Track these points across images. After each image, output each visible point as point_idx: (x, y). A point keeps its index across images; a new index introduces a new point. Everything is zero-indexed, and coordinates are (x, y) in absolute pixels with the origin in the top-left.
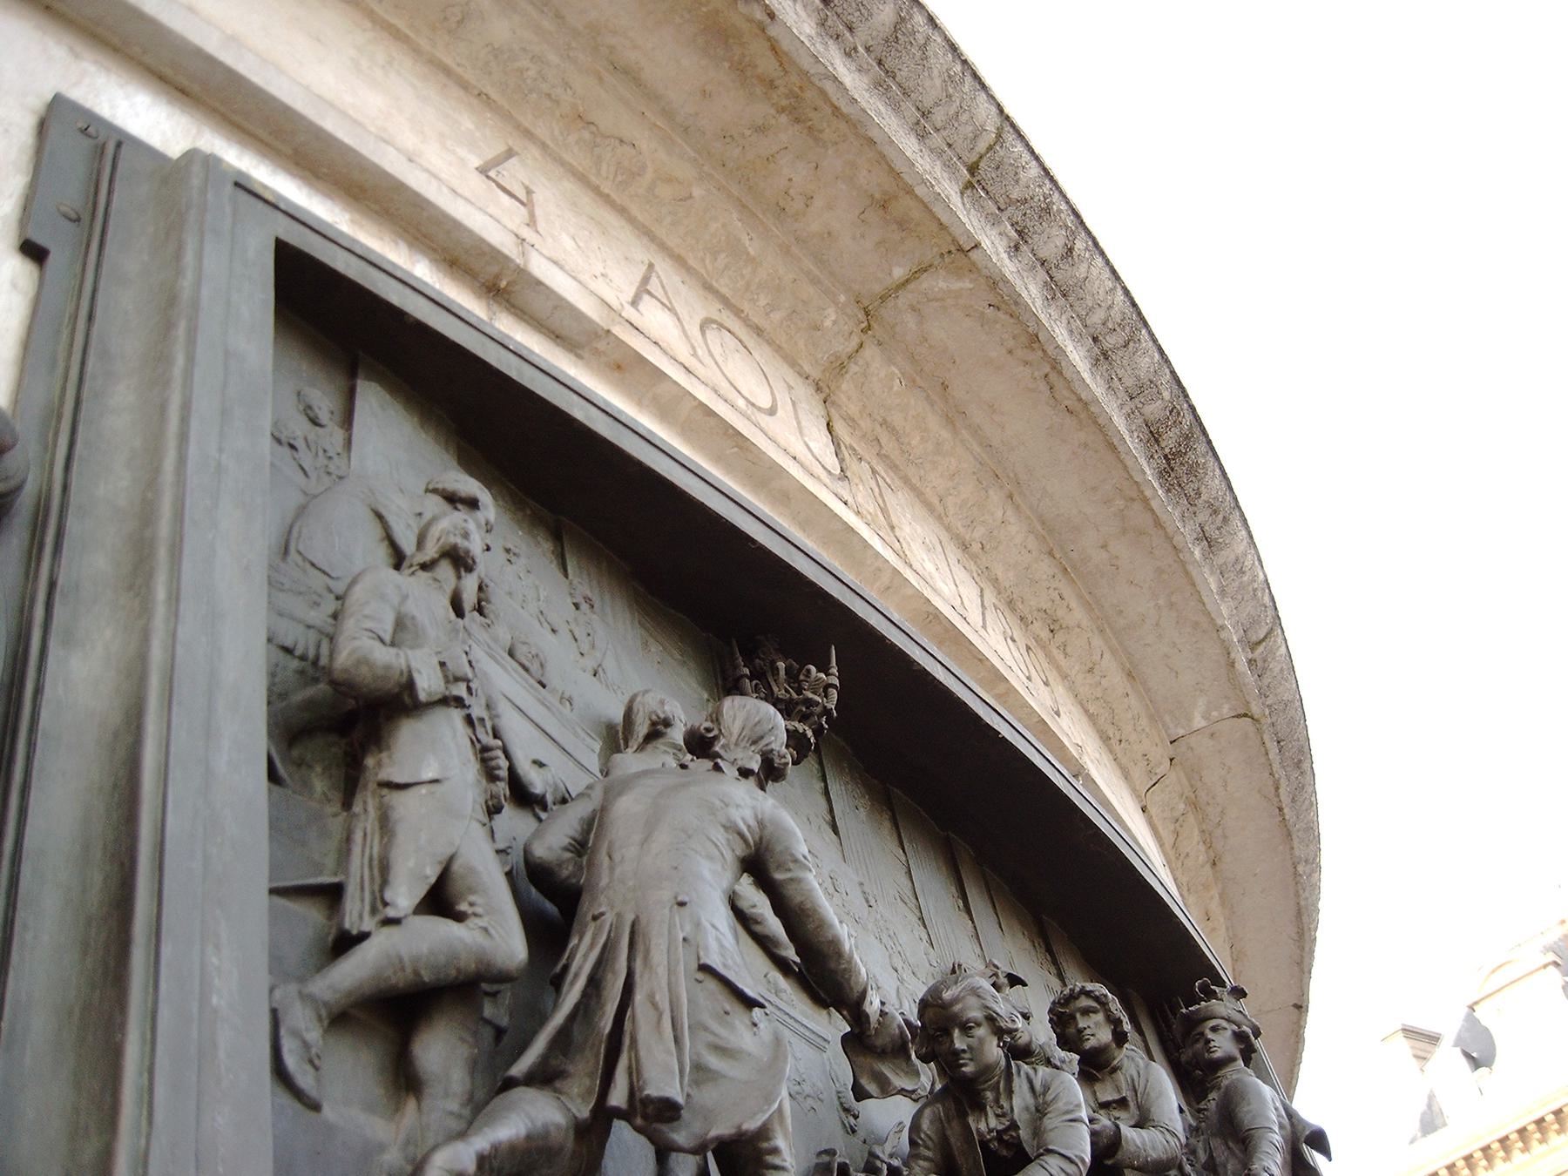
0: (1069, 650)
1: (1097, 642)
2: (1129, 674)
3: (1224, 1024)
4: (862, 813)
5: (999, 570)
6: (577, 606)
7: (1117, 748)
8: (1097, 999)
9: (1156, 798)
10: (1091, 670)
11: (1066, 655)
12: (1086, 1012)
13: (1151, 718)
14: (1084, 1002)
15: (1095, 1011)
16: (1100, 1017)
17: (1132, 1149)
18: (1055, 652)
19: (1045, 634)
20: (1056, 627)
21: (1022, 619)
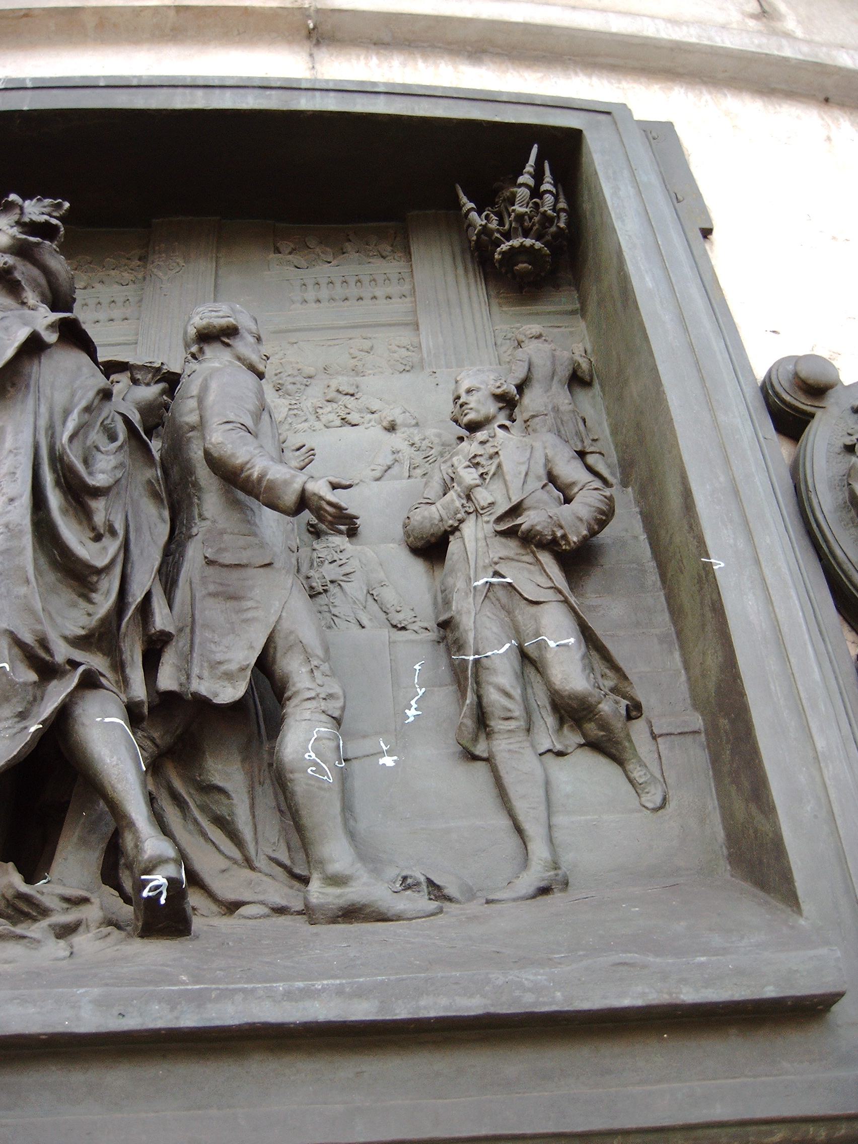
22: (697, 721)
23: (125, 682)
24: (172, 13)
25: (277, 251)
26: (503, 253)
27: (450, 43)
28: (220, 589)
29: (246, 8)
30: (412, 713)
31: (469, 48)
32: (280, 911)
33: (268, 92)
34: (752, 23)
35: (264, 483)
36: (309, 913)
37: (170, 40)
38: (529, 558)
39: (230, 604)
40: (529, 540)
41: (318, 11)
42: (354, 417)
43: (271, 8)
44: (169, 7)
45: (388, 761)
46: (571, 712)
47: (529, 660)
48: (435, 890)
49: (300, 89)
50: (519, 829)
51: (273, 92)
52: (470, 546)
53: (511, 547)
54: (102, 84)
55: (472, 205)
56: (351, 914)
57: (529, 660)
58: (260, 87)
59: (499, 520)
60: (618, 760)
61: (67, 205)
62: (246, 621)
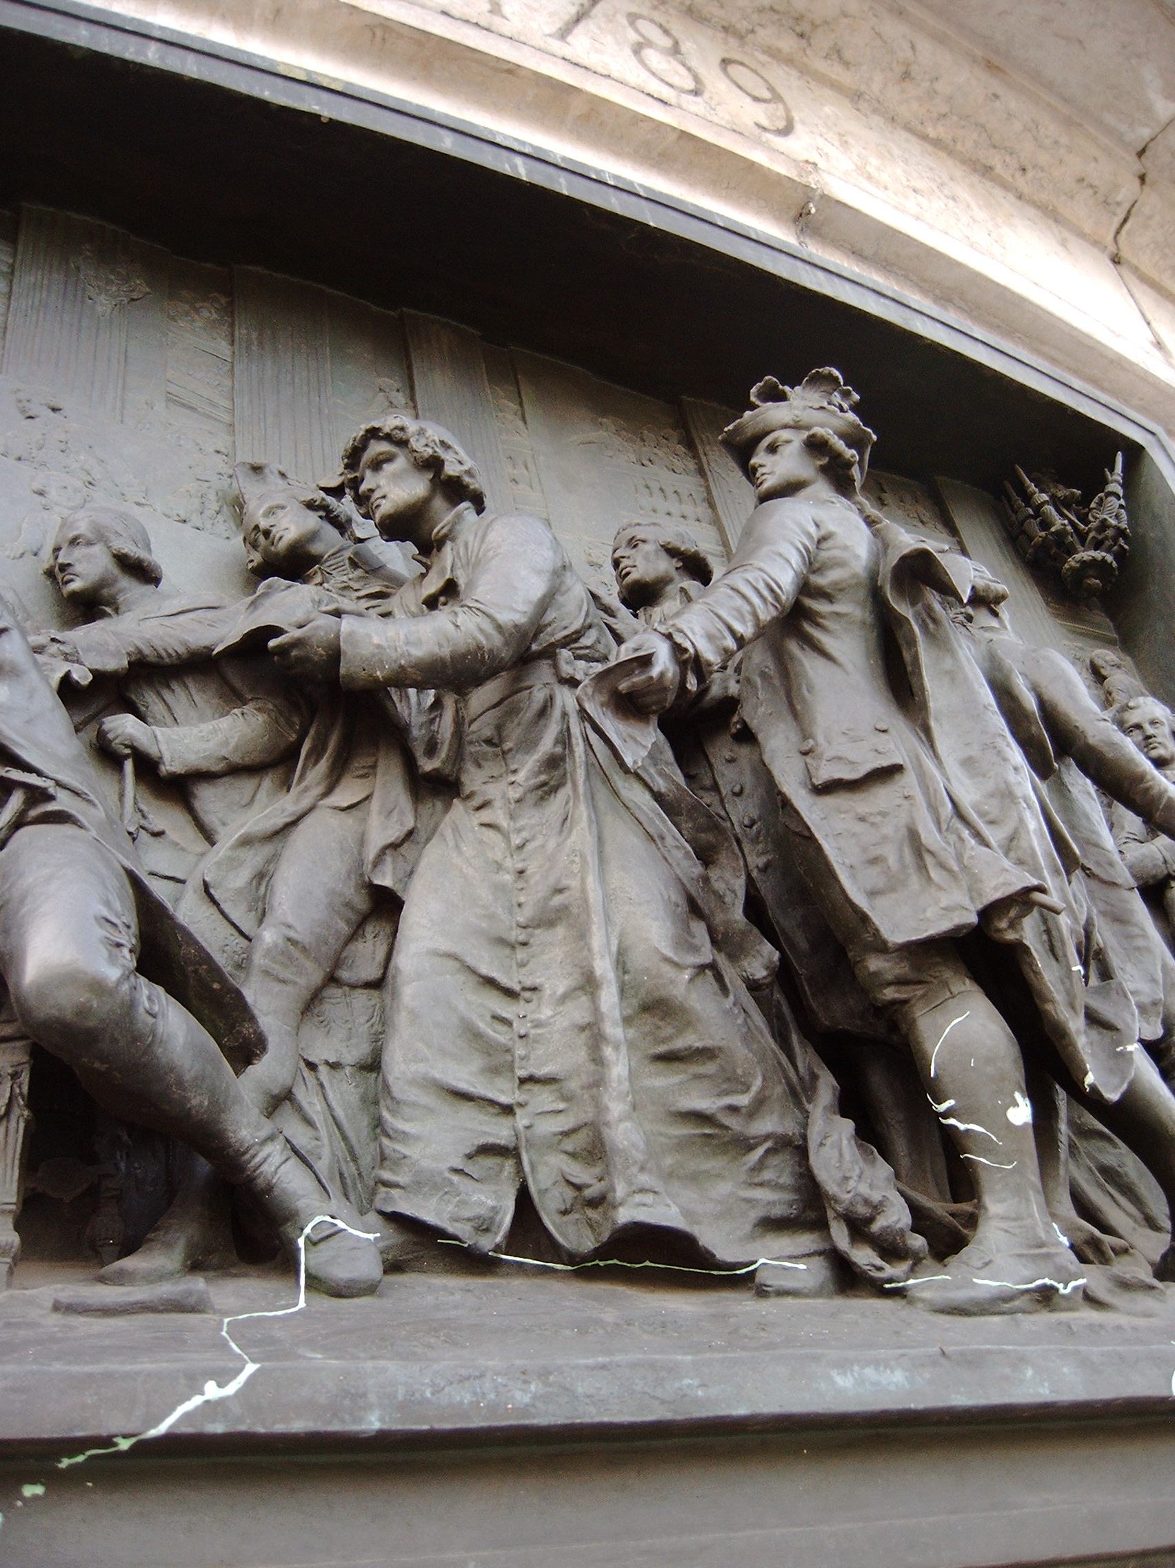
0: (848, 54)
1: (893, 29)
2: (990, 66)
3: (784, 435)
4: (103, 304)
7: (1021, 182)
8: (388, 438)
9: (1136, 244)
10: (906, 76)
11: (847, 65)
12: (377, 465)
13: (1068, 122)
14: (377, 448)
15: (390, 459)
16: (401, 462)
17: (366, 651)
18: (820, 65)
19: (787, 43)
20: (805, 27)
21: (726, 29)
24: (673, 137)
26: (1083, 562)
27: (925, 281)
28: (1109, 908)
29: (753, 163)
31: (937, 292)
33: (882, 300)
35: (1164, 801)
37: (653, 166)
39: (1116, 926)
41: (824, 197)
43: (778, 174)
44: (674, 129)
49: (909, 307)
51: (887, 302)
54: (720, 223)
55: (1045, 497)
58: (874, 291)
61: (856, 397)
62: (1138, 949)
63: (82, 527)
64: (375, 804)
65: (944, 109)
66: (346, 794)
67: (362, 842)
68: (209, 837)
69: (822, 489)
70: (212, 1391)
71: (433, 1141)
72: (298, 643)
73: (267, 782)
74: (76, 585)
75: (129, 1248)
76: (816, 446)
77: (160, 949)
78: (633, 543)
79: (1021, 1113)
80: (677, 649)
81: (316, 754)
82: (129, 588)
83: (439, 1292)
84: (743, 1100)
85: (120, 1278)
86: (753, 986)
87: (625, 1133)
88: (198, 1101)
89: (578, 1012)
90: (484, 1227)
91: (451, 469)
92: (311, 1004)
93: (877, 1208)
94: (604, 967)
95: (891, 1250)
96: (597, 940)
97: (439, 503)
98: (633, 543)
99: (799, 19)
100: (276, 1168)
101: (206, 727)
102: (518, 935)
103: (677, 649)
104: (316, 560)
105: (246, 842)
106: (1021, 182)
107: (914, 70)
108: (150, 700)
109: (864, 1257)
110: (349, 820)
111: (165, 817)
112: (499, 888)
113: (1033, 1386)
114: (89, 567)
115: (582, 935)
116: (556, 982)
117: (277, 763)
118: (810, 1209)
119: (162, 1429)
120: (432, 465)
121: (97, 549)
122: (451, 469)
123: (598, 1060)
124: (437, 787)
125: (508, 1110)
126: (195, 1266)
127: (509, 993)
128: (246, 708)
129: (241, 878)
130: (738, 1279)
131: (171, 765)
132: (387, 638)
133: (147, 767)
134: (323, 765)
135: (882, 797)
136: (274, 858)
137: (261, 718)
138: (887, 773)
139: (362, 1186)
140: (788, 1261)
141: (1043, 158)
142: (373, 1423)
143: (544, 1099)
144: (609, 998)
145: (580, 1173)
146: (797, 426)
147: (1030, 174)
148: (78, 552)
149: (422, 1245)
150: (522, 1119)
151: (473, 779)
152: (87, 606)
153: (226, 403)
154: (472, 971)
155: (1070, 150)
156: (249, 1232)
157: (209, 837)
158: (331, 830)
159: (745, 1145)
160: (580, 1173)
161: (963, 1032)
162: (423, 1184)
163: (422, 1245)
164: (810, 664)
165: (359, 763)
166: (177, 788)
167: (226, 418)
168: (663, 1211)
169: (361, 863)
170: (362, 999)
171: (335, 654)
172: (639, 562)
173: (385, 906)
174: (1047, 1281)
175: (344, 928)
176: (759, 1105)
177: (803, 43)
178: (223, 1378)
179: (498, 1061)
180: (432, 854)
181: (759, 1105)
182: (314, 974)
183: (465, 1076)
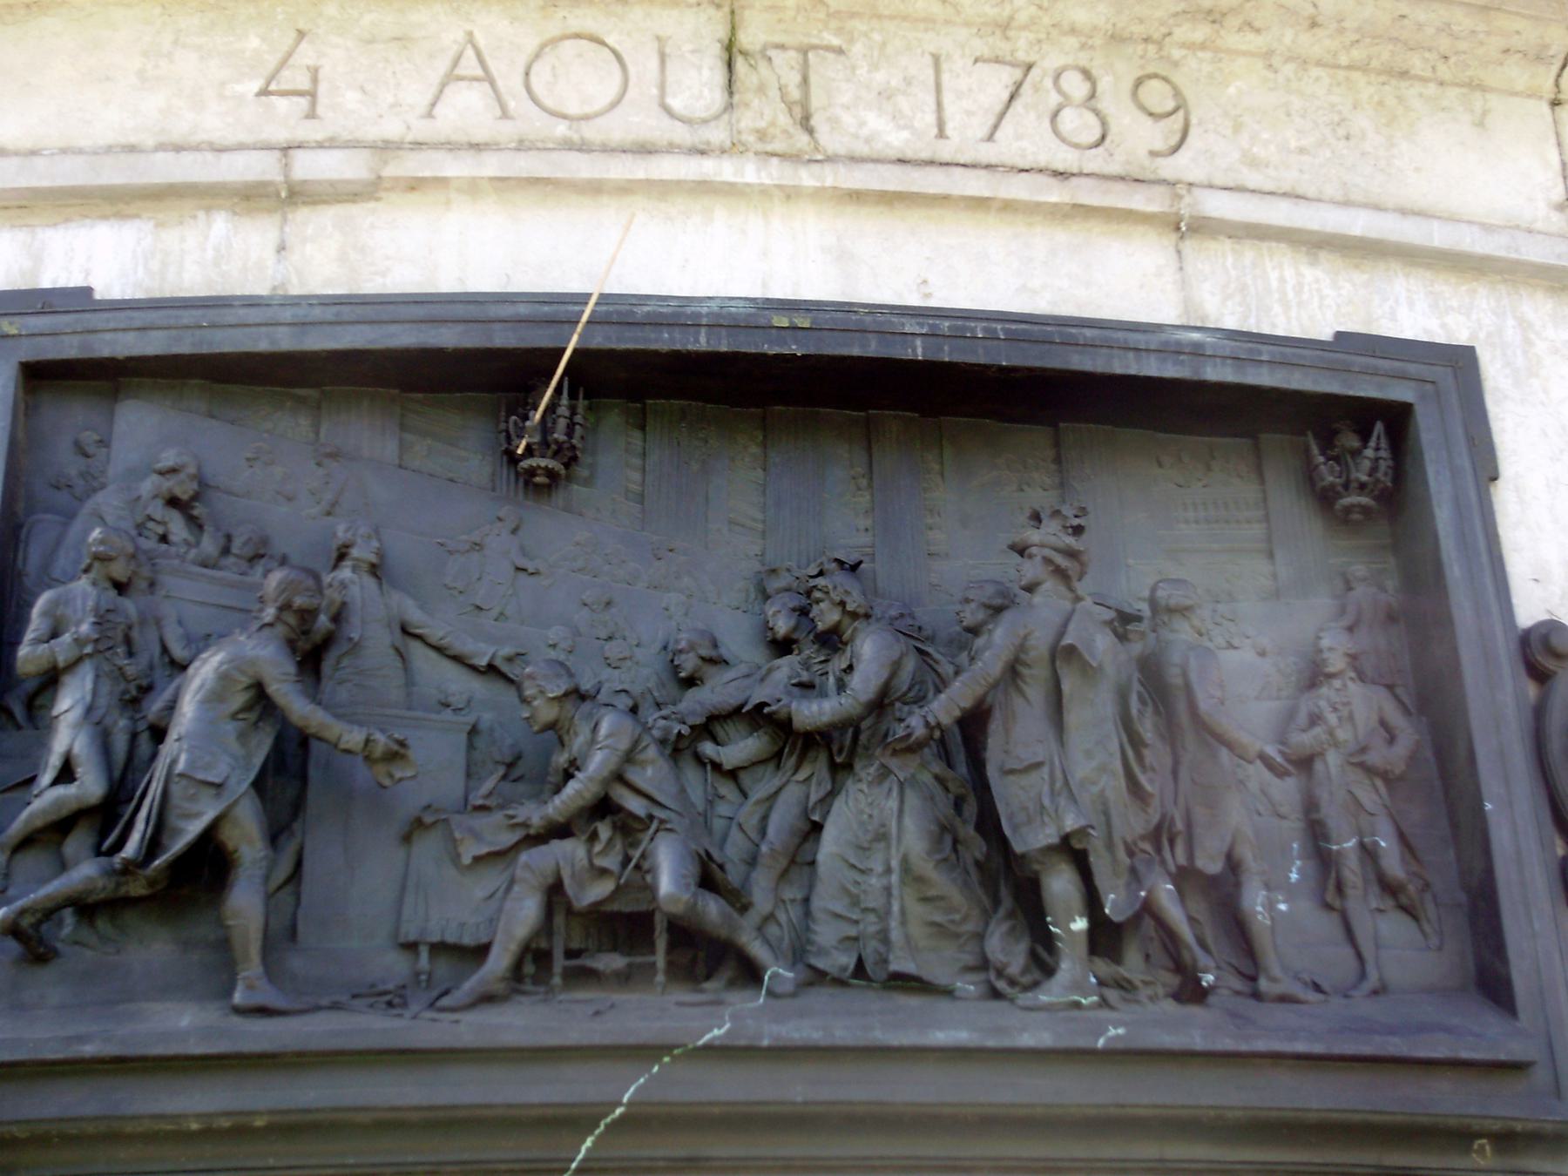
0: (1257, 24)
5: (1081, 16)
6: (319, 464)
7: (1444, 71)
10: (1314, 24)
11: (1258, 31)
20: (1217, 16)
22: (1462, 897)
23: (1163, 862)
25: (1160, 465)
30: (1294, 876)
32: (1238, 993)
34: (1556, 217)
36: (1257, 996)
38: (1367, 782)
40: (1369, 770)
42: (1236, 642)
45: (1283, 907)
46: (1390, 888)
47: (1369, 853)
48: (1317, 988)
50: (1359, 956)
52: (1333, 770)
53: (1355, 775)
56: (1284, 999)
57: (1369, 853)
59: (1351, 755)
60: (1415, 918)
63: (683, 645)
64: (814, 780)
65: (1357, 37)
66: (801, 776)
67: (808, 797)
68: (745, 795)
69: (1050, 585)
70: (716, 1032)
71: (826, 933)
72: (774, 713)
73: (771, 766)
74: (683, 675)
75: (708, 977)
76: (1048, 561)
77: (708, 878)
78: (967, 601)
79: (1080, 924)
80: (927, 724)
81: (791, 753)
82: (709, 670)
83: (821, 997)
84: (957, 917)
85: (702, 991)
86: (978, 864)
87: (896, 935)
88: (723, 933)
89: (884, 881)
90: (844, 969)
91: (849, 608)
92: (784, 874)
93: (1006, 966)
94: (895, 863)
95: (1012, 983)
96: (893, 851)
97: (847, 621)
98: (967, 601)
99: (1210, 12)
100: (757, 950)
101: (742, 744)
102: (866, 845)
103: (927, 724)
104: (795, 641)
105: (758, 802)
106: (1444, 71)
107: (1320, 19)
108: (718, 730)
109: (1001, 985)
110: (804, 788)
111: (726, 789)
112: (861, 824)
113: (1027, 1040)
114: (688, 664)
115: (888, 847)
116: (879, 868)
117: (776, 758)
118: (984, 964)
119: (701, 1042)
120: (842, 604)
121: (691, 655)
122: (849, 608)
123: (889, 903)
124: (841, 769)
125: (856, 922)
126: (731, 984)
127: (862, 872)
128: (761, 732)
129: (755, 820)
130: (948, 993)
131: (727, 766)
132: (812, 712)
133: (717, 767)
134: (793, 760)
135: (1034, 777)
136: (770, 808)
137: (765, 739)
138: (1037, 766)
139: (799, 953)
140: (968, 986)
141: (1462, 45)
142: (765, 1043)
143: (872, 918)
144: (895, 878)
145: (882, 949)
146: (1042, 546)
147: (1453, 60)
148: (683, 657)
149: (819, 977)
150: (861, 926)
151: (858, 766)
152: (691, 682)
153: (760, 516)
154: (847, 861)
155: (1488, 33)
156: (750, 974)
157: (745, 795)
158: (795, 789)
159: (957, 936)
160: (882, 949)
161: (1060, 884)
162: (822, 952)
163: (819, 977)
164: (1018, 701)
165: (811, 754)
166: (733, 774)
167: (760, 526)
168: (909, 967)
169: (806, 808)
170: (806, 869)
171: (790, 720)
172: (968, 615)
173: (817, 828)
174: (1076, 998)
175: (797, 841)
176: (965, 919)
177: (1216, 26)
178: (720, 1028)
179: (855, 902)
180: (839, 804)
181: (965, 919)
182: (784, 862)
183: (839, 908)
